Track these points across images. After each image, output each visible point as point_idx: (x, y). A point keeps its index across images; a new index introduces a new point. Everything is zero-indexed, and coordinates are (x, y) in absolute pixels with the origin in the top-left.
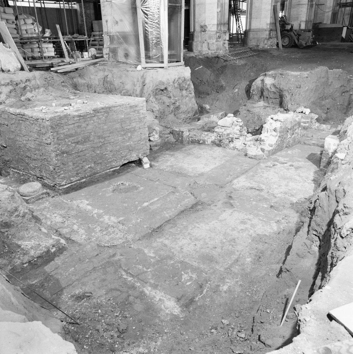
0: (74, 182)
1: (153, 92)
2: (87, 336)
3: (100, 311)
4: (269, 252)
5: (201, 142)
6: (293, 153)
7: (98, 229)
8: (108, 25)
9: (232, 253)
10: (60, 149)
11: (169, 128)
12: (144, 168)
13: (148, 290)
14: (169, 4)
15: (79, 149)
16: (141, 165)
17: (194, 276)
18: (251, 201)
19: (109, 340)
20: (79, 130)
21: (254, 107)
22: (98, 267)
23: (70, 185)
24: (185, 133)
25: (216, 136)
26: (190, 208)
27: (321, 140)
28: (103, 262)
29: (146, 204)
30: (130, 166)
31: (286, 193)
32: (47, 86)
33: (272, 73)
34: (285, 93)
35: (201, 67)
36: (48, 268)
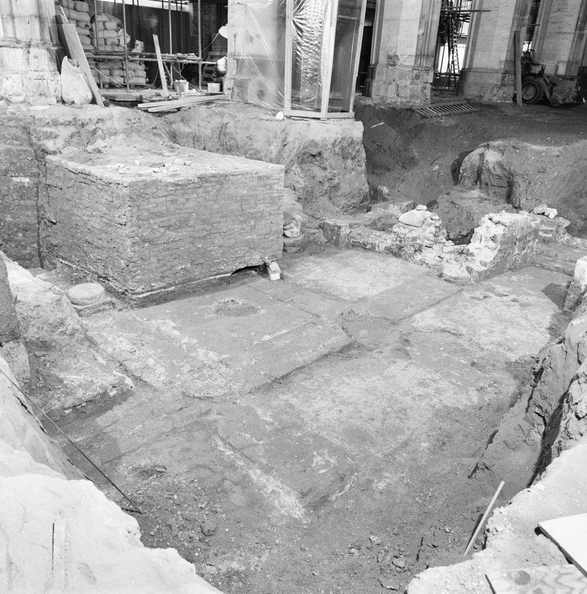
0: (156, 290)
1: (298, 158)
2: (152, 533)
3: (175, 497)
4: (461, 437)
5: (367, 247)
6: (520, 280)
7: (187, 368)
8: (236, 41)
9: (400, 431)
10: (140, 235)
11: (318, 218)
12: (270, 280)
13: (255, 474)
14: (340, 16)
15: (169, 238)
16: (266, 275)
17: (333, 461)
18: (440, 350)
19: (186, 544)
20: (172, 208)
21: (462, 198)
22: (181, 428)
23: (149, 293)
24: (343, 229)
25: (395, 239)
26: (338, 352)
27: (570, 264)
28: (189, 422)
29: (267, 337)
30: (249, 275)
31: (500, 345)
32: (129, 132)
33: (499, 144)
34: (518, 180)
35: (383, 123)
36: (101, 421)
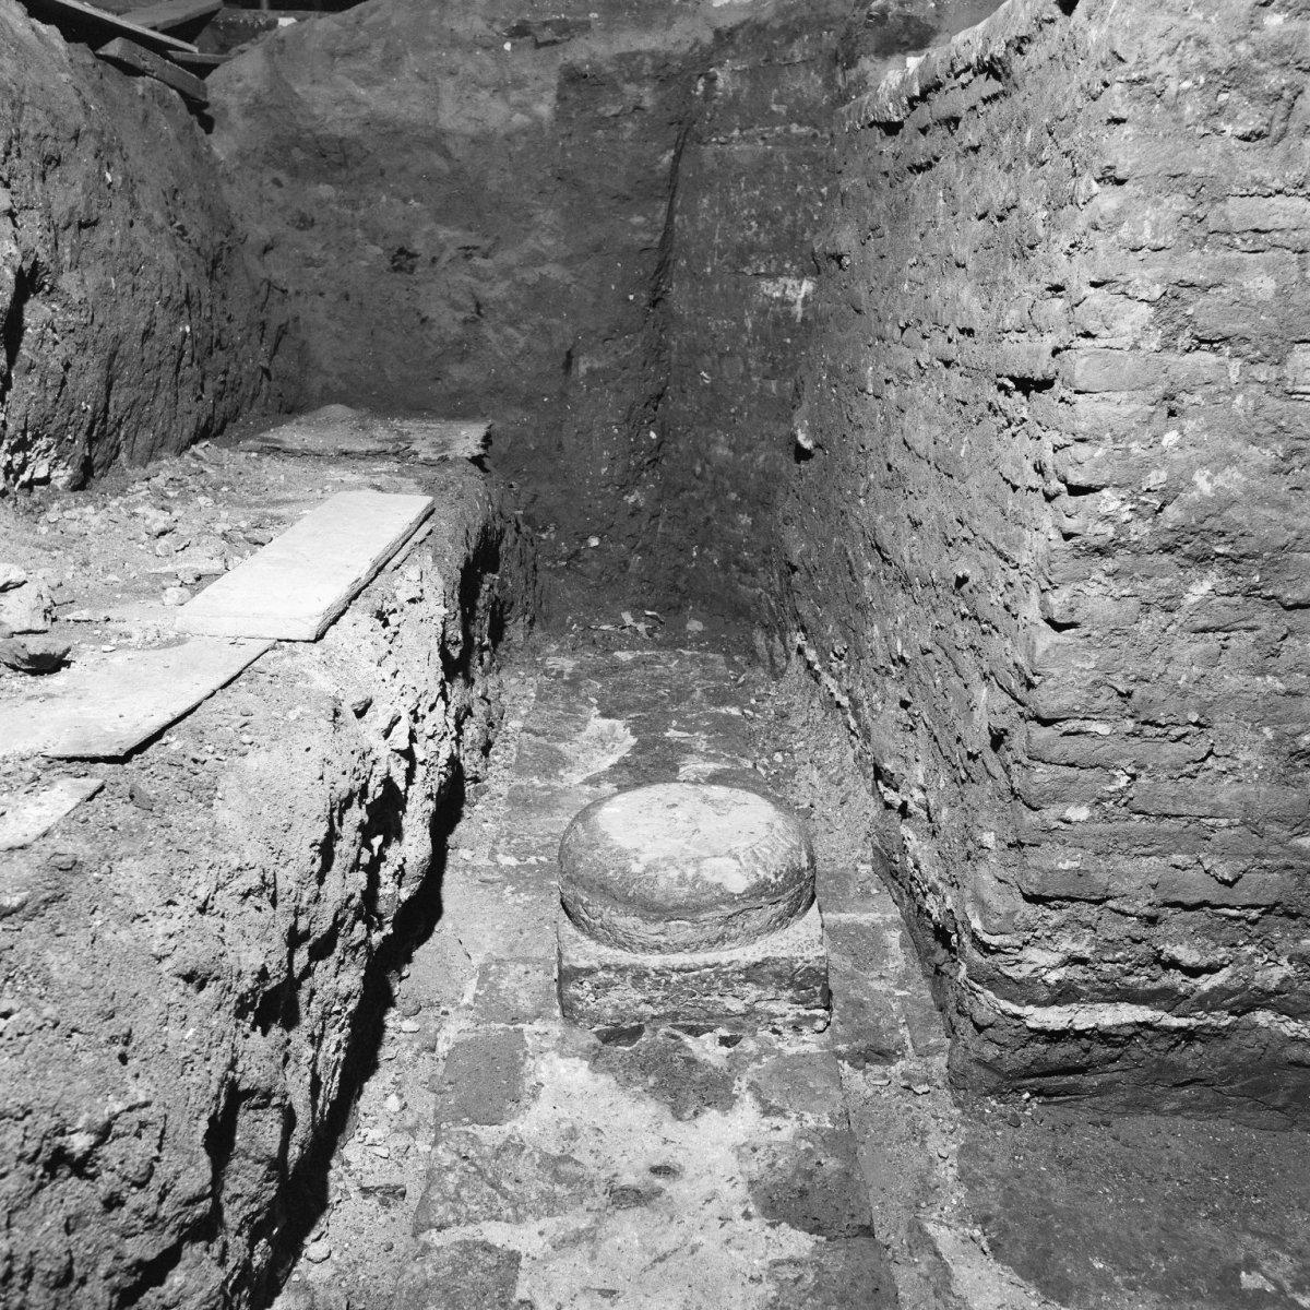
10: (1156, 478)
